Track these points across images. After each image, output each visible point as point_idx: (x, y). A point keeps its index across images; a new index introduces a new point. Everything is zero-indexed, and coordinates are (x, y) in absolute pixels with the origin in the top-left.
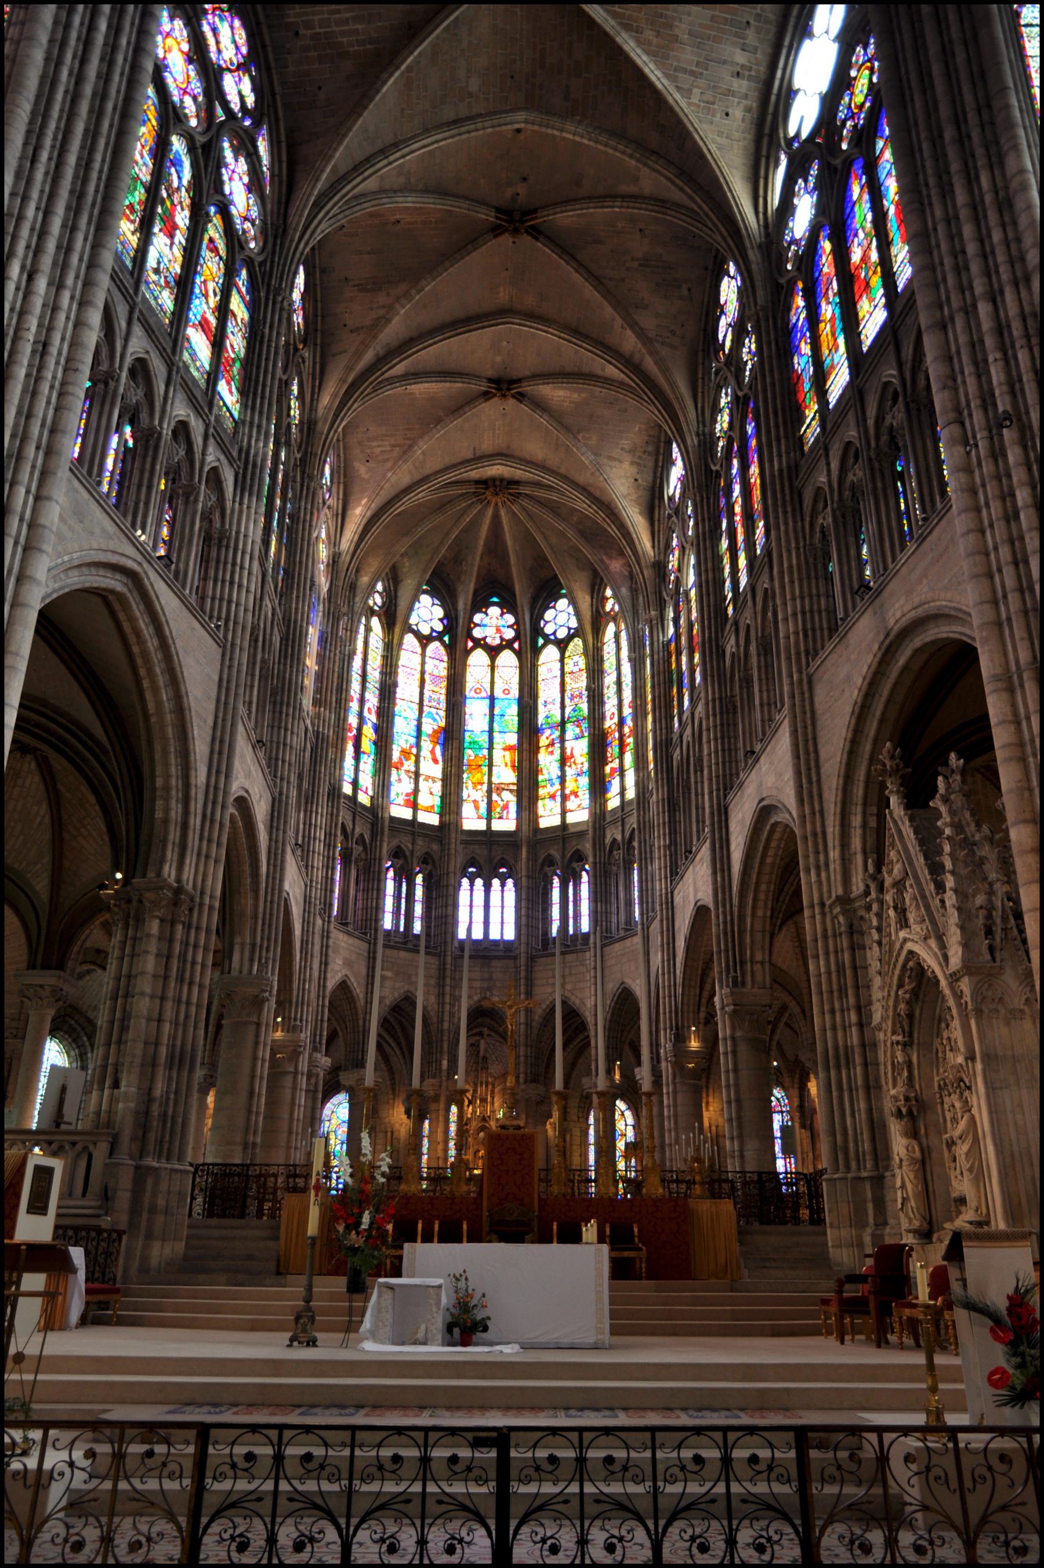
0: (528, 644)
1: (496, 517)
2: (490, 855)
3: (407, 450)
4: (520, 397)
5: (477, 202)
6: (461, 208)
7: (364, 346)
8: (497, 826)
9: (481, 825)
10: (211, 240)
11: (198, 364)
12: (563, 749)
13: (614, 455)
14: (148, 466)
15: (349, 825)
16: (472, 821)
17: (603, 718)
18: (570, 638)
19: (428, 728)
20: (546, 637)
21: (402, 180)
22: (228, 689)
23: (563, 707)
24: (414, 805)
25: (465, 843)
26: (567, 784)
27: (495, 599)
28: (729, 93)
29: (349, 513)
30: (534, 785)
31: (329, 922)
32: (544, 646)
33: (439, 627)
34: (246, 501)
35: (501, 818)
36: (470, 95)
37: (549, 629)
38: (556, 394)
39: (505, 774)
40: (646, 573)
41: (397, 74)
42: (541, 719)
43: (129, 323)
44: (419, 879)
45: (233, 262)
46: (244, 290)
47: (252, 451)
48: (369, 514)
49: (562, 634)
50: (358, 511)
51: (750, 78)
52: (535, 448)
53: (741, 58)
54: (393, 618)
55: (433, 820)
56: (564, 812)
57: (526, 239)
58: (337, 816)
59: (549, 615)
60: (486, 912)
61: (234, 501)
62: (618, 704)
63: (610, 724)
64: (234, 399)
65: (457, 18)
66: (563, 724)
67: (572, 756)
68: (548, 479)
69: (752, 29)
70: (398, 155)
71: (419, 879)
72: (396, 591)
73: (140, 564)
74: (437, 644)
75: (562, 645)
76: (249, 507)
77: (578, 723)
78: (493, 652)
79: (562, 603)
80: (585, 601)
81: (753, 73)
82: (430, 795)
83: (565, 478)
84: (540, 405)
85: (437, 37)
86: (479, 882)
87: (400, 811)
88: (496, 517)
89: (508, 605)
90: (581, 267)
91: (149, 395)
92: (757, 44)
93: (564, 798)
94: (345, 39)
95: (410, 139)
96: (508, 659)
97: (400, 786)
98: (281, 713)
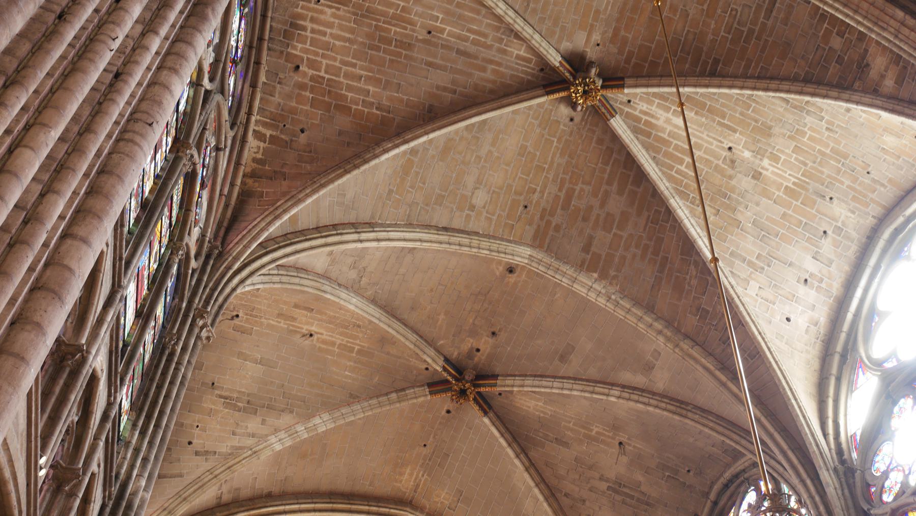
5: (426, 341)
6: (407, 340)
21: (353, 275)
28: (793, 298)
36: (472, 208)
41: (403, 148)
51: (819, 289)
53: (811, 266)
57: (472, 411)
65: (484, 121)
69: (829, 240)
70: (372, 235)
81: (823, 285)
85: (457, 132)
90: (532, 466)
92: (832, 257)
94: (350, 95)
95: (389, 226)
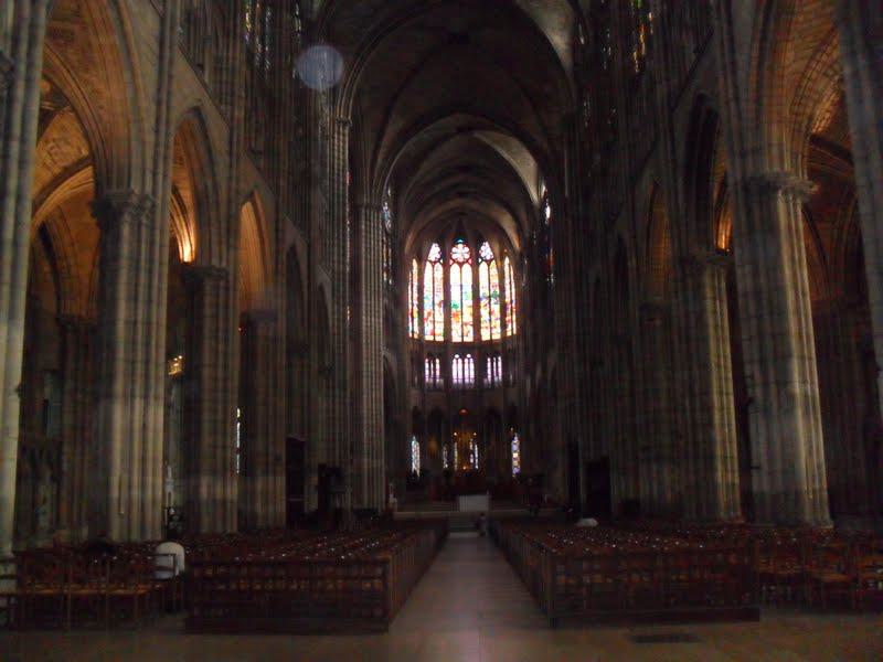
0: (475, 259)
2: (463, 349)
8: (466, 339)
9: (459, 340)
16: (456, 338)
18: (491, 260)
19: (437, 301)
24: (434, 334)
30: (480, 322)
33: (439, 256)
37: (483, 255)
39: (468, 318)
42: (481, 295)
44: (437, 361)
49: (488, 258)
54: (422, 259)
55: (440, 339)
59: (483, 248)
60: (463, 370)
62: (511, 293)
63: (508, 300)
66: (490, 297)
71: (437, 361)
75: (489, 262)
78: (461, 264)
79: (487, 244)
82: (440, 329)
86: (460, 361)
87: (429, 337)
89: (466, 243)
96: (467, 268)
97: (428, 327)
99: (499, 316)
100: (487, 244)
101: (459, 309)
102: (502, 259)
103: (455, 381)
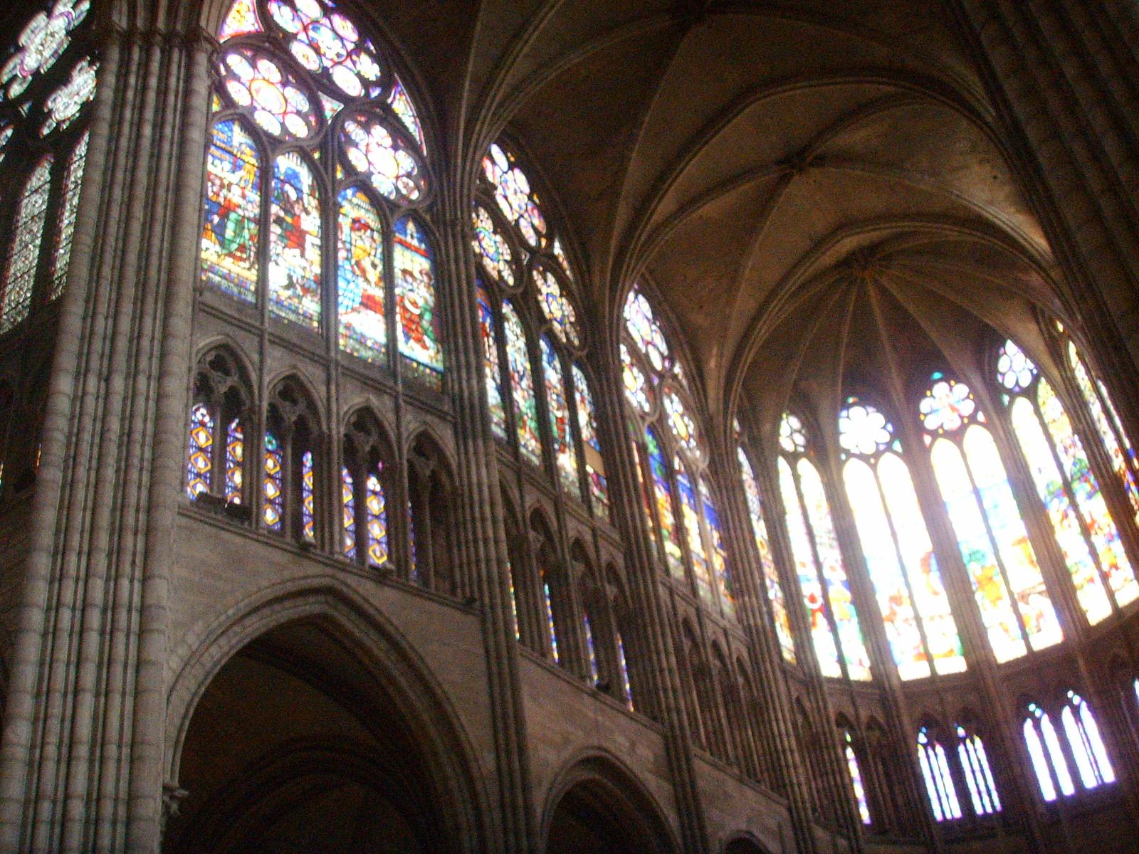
1: (883, 291)
3: (734, 279)
4: (820, 161)
7: (612, 208)
10: (355, 221)
11: (369, 343)
12: (1080, 517)
13: (955, 164)
14: (325, 474)
15: (849, 711)
17: (1108, 459)
20: (1010, 392)
22: (499, 658)
23: (1060, 466)
25: (1007, 678)
26: (1102, 558)
27: (937, 375)
29: (705, 370)
31: (857, 838)
32: (1011, 402)
33: (886, 437)
34: (471, 449)
35: (1039, 630)
37: (1009, 383)
38: (856, 137)
40: (1053, 274)
42: (1042, 493)
43: (261, 353)
45: (388, 225)
46: (415, 243)
47: (466, 394)
48: (725, 362)
49: (1026, 381)
50: (712, 364)
52: (873, 202)
56: (1111, 595)
58: (826, 708)
59: (1003, 364)
61: (458, 454)
64: (432, 352)
67: (1094, 522)
68: (906, 226)
72: (816, 420)
73: (333, 577)
74: (888, 455)
75: (1030, 393)
76: (476, 453)
77: (1083, 478)
78: (956, 436)
79: (1010, 346)
80: (1031, 331)
83: (921, 216)
84: (844, 158)
87: (910, 669)
88: (883, 291)
89: (951, 375)
91: (311, 405)
93: (1105, 577)
96: (980, 439)
98: (646, 637)
99: (1114, 530)
100: (1010, 346)
101: (991, 560)
102: (1059, 358)
103: (1049, 795)
